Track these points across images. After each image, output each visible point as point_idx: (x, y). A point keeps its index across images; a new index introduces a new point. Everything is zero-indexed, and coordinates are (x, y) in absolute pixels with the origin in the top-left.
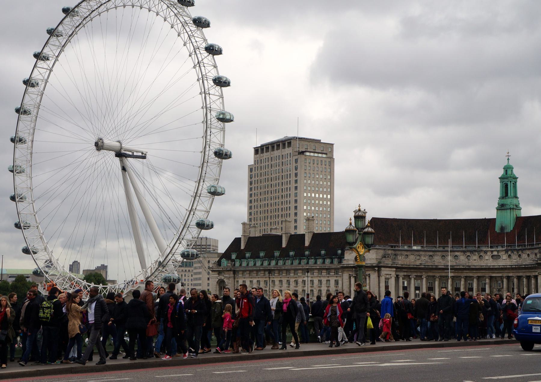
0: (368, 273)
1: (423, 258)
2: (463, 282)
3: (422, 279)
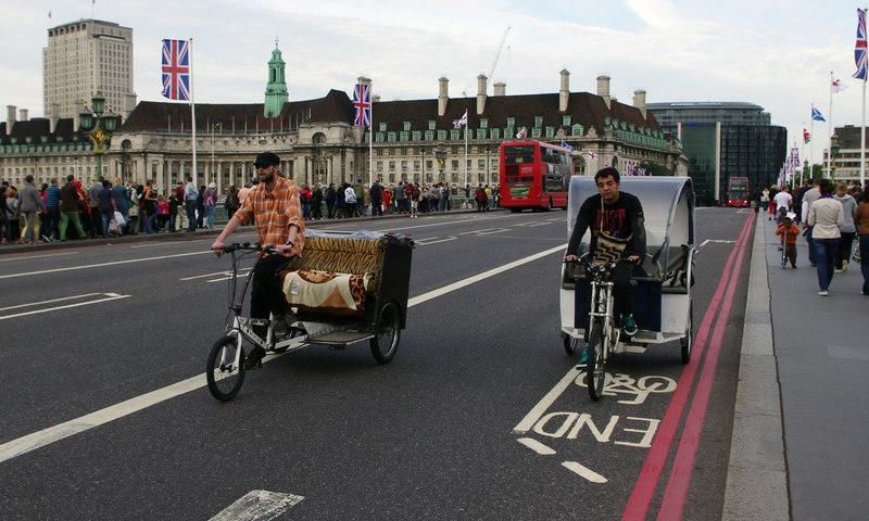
0: (134, 159)
2: (231, 168)
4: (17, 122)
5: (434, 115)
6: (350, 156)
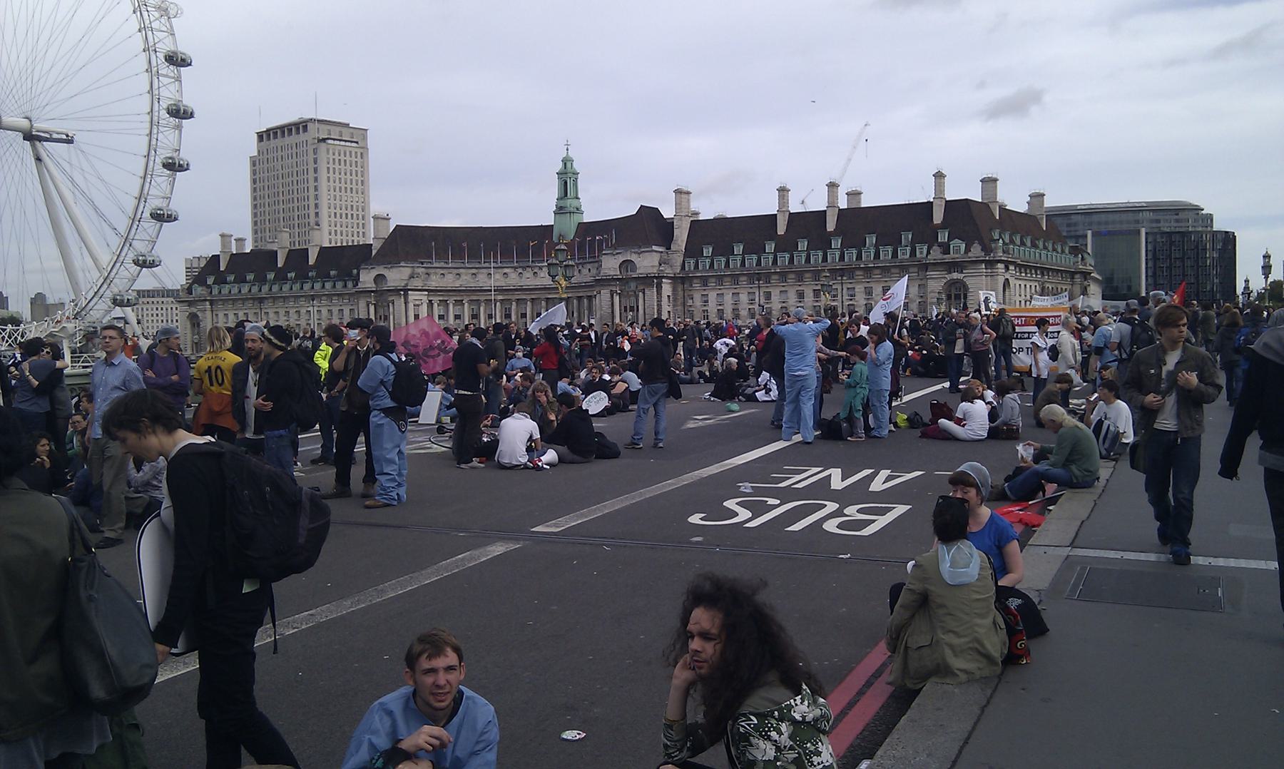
0: (391, 299)
1: (464, 277)
3: (464, 304)
4: (233, 254)
5: (772, 235)
6: (667, 289)
